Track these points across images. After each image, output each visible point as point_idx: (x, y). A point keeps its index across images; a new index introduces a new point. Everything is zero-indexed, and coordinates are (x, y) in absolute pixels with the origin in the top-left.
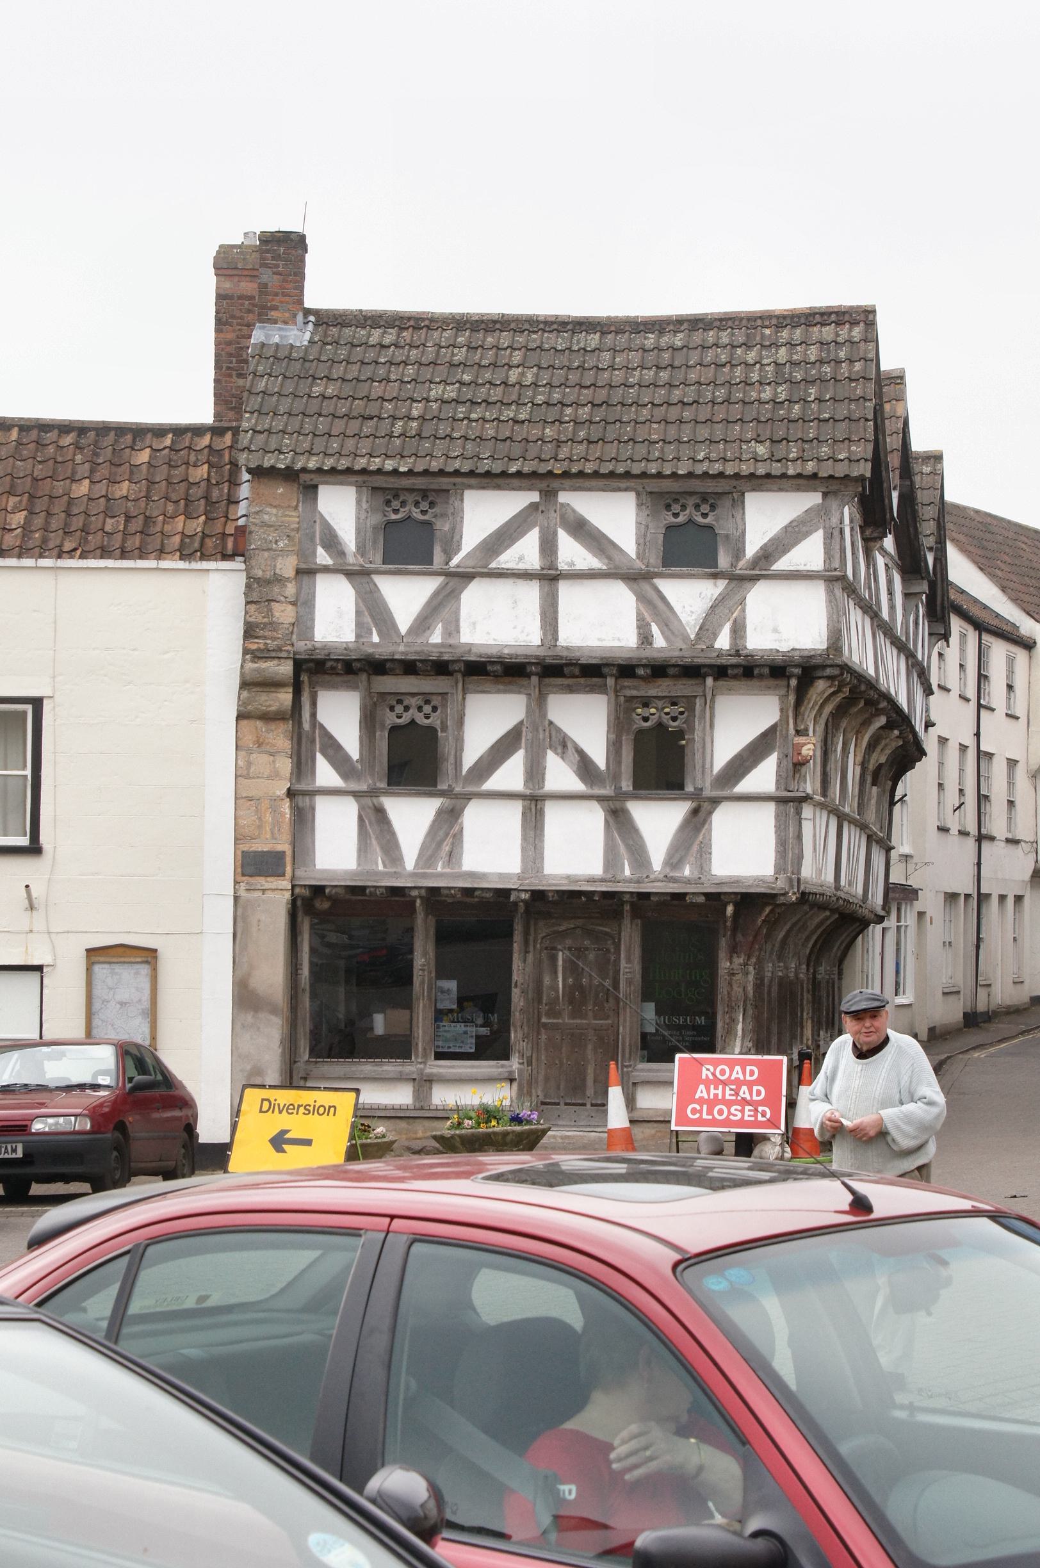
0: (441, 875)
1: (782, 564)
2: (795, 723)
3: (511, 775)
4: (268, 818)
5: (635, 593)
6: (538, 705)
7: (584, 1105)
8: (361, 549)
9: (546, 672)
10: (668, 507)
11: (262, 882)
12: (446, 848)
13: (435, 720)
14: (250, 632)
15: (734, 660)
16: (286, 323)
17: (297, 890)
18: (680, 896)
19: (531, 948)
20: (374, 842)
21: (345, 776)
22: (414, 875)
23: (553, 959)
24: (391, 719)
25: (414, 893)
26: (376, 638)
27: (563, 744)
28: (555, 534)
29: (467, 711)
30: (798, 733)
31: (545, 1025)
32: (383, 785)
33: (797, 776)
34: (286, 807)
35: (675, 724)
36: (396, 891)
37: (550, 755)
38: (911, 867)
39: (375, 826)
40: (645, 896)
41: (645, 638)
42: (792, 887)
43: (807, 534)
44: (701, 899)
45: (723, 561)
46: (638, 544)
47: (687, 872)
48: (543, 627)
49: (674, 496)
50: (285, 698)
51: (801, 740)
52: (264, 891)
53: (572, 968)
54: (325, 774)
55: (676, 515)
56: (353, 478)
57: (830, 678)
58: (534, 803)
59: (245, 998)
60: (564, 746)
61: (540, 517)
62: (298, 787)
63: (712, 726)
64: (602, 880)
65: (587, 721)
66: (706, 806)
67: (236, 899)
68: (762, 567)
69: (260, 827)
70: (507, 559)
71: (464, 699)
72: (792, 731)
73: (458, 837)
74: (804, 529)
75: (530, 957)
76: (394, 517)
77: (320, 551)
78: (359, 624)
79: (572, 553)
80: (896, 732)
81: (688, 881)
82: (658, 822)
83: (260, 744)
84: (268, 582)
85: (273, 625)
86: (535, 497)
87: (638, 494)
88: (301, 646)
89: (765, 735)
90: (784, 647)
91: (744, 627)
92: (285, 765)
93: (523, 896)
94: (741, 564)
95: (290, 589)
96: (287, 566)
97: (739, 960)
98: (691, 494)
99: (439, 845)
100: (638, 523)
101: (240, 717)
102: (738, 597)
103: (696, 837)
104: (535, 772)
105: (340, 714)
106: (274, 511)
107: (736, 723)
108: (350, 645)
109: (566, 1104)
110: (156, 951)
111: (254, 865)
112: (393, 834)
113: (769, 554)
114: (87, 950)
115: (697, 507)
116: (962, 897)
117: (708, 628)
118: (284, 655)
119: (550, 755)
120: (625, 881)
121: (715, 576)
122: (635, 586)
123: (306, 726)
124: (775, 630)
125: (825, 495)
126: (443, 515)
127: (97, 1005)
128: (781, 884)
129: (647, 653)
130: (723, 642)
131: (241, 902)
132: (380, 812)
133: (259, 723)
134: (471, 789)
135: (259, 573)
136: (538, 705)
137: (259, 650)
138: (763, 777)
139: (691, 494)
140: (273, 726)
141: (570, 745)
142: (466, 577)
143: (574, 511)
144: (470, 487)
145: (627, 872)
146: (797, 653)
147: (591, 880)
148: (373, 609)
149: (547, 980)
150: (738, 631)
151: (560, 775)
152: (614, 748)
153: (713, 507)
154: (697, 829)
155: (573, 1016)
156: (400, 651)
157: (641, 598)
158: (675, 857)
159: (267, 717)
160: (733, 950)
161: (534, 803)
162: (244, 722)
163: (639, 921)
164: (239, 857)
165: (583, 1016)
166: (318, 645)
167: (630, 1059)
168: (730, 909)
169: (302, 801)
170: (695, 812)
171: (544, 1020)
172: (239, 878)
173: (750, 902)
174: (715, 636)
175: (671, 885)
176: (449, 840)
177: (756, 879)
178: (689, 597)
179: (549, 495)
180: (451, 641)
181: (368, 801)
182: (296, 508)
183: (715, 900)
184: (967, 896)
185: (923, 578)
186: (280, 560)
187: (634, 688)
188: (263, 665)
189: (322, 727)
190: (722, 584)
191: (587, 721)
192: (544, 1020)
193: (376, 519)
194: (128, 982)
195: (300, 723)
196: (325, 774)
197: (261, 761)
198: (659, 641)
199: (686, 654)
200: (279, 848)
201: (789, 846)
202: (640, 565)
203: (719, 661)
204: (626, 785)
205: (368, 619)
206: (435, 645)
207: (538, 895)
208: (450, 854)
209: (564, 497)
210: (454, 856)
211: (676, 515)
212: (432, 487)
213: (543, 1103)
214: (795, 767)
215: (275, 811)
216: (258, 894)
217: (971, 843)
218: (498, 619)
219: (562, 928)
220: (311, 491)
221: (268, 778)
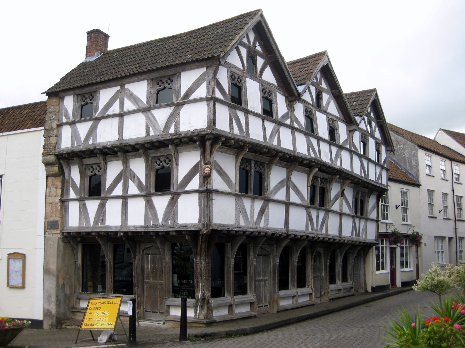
0: (99, 227)
1: (192, 97)
2: (204, 160)
3: (118, 191)
4: (54, 209)
5: (145, 117)
6: (126, 163)
7: (157, 312)
8: (74, 116)
9: (124, 150)
10: (158, 84)
11: (53, 231)
12: (101, 218)
13: (101, 174)
14: (44, 146)
15: (174, 137)
16: (92, 56)
17: (64, 234)
18: (168, 232)
19: (138, 254)
20: (83, 216)
21: (76, 194)
22: (93, 227)
23: (147, 258)
24: (89, 173)
25: (93, 234)
26: (76, 145)
27: (134, 177)
28: (124, 99)
29: (108, 168)
30: (206, 164)
31: (145, 282)
32: (86, 196)
33: (206, 182)
34: (59, 206)
35: (167, 166)
36: (89, 233)
37: (130, 181)
38: (409, 228)
39: (83, 210)
40: (158, 232)
41: (148, 132)
42: (204, 227)
43: (201, 84)
44: (174, 233)
45: (174, 100)
46: (147, 98)
47: (169, 223)
48: (119, 134)
49: (160, 79)
50: (56, 169)
51: (204, 166)
52: (53, 234)
53: (153, 262)
54: (72, 195)
55: (160, 86)
56: (72, 92)
57: (209, 139)
58: (125, 198)
59: (47, 271)
60: (134, 178)
61: (120, 95)
62: (65, 198)
63: (177, 164)
64: (144, 227)
65: (139, 167)
66: (176, 196)
67: (45, 237)
68: (186, 100)
69: (52, 213)
70: (110, 112)
71: (106, 163)
72: (203, 164)
73: (104, 213)
74: (200, 82)
75: (137, 257)
76: (83, 103)
77: (64, 118)
78: (72, 141)
79: (129, 105)
80: (338, 176)
81: (170, 227)
82: (161, 203)
83: (53, 185)
84: (50, 130)
85: (50, 144)
86: (118, 88)
87: (148, 80)
88: (58, 151)
89: (195, 166)
90: (192, 129)
91: (179, 123)
92: (59, 191)
93: (122, 234)
94: (179, 99)
95: (55, 132)
96: (54, 125)
97: (199, 258)
98: (165, 77)
99: (99, 217)
100: (147, 91)
101: (47, 177)
102: (177, 113)
103: (173, 209)
104: (125, 188)
105: (75, 174)
106: (52, 107)
107: (187, 161)
108: (70, 148)
109: (153, 312)
110: (24, 255)
111: (50, 225)
112: (88, 213)
113: (187, 95)
114: (8, 254)
115: (167, 83)
116: (447, 239)
117: (167, 126)
118: (51, 153)
119: (130, 181)
120: (151, 227)
121: (169, 105)
122: (145, 113)
123: (67, 178)
124: (190, 123)
125: (207, 68)
126: (95, 100)
127: (10, 272)
128: (201, 227)
129: (149, 139)
130: (172, 130)
131: (46, 238)
132: (85, 205)
133: (53, 178)
134: (108, 196)
135: (47, 128)
136: (126, 163)
137: (46, 153)
138: (195, 184)
139: (165, 77)
140: (57, 178)
141: (136, 177)
142: (98, 119)
143: (129, 91)
144: (101, 89)
145: (151, 224)
146: (197, 131)
147: (141, 227)
148: (75, 135)
149: (146, 266)
150: (177, 126)
151: (133, 189)
152: (148, 176)
153: (172, 81)
154: (173, 206)
155: (153, 279)
156: (82, 148)
157: (148, 118)
158: (166, 218)
159: (55, 175)
160: (197, 253)
161: (125, 198)
162: (49, 178)
163: (169, 243)
164: (46, 223)
165: (156, 280)
166: (62, 149)
167: (166, 296)
168: (187, 237)
169: (66, 203)
170: (172, 199)
171: (145, 280)
172: (47, 230)
173: (194, 234)
174: (170, 128)
175: (165, 228)
176: (102, 215)
177: (192, 224)
178: (161, 115)
179: (122, 86)
180: (94, 143)
181: (82, 202)
182: (59, 105)
183: (179, 232)
184: (450, 239)
185: (354, 125)
186: (53, 123)
187: (153, 153)
188: (46, 158)
189: (72, 178)
190: (172, 108)
191: (139, 167)
192: (145, 280)
193: (79, 104)
194: (17, 265)
195: (64, 177)
196: (72, 195)
197: (53, 190)
198: (152, 133)
199: (160, 137)
200: (57, 219)
201: (206, 210)
202: (147, 106)
203: (171, 138)
204: (153, 191)
205: (74, 139)
206: (90, 145)
207: (126, 233)
208: (103, 220)
209: (127, 86)
210: (103, 220)
211: (160, 86)
212: (92, 91)
213: (146, 311)
214: (206, 178)
215: (56, 207)
216: (51, 235)
217: (452, 223)
218: (107, 134)
219: (147, 246)
220: (62, 99)
221: (55, 196)
